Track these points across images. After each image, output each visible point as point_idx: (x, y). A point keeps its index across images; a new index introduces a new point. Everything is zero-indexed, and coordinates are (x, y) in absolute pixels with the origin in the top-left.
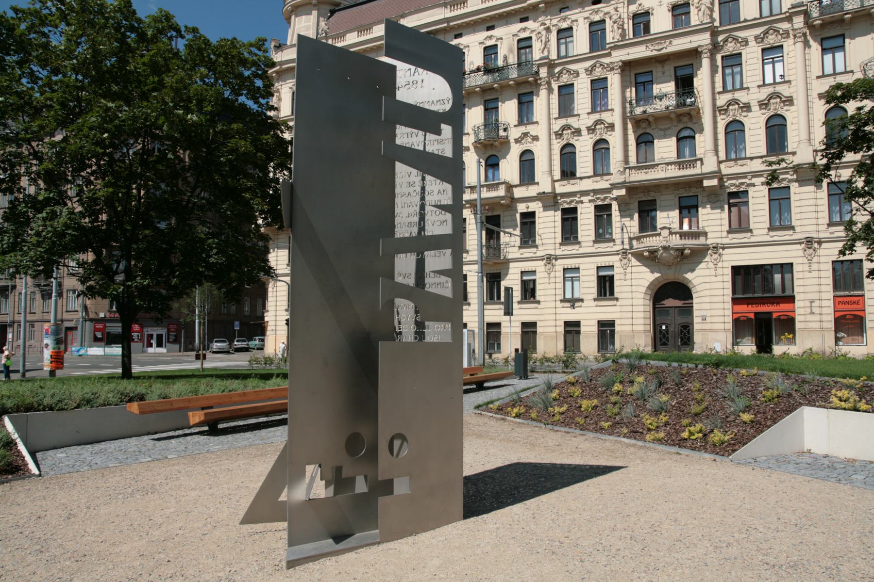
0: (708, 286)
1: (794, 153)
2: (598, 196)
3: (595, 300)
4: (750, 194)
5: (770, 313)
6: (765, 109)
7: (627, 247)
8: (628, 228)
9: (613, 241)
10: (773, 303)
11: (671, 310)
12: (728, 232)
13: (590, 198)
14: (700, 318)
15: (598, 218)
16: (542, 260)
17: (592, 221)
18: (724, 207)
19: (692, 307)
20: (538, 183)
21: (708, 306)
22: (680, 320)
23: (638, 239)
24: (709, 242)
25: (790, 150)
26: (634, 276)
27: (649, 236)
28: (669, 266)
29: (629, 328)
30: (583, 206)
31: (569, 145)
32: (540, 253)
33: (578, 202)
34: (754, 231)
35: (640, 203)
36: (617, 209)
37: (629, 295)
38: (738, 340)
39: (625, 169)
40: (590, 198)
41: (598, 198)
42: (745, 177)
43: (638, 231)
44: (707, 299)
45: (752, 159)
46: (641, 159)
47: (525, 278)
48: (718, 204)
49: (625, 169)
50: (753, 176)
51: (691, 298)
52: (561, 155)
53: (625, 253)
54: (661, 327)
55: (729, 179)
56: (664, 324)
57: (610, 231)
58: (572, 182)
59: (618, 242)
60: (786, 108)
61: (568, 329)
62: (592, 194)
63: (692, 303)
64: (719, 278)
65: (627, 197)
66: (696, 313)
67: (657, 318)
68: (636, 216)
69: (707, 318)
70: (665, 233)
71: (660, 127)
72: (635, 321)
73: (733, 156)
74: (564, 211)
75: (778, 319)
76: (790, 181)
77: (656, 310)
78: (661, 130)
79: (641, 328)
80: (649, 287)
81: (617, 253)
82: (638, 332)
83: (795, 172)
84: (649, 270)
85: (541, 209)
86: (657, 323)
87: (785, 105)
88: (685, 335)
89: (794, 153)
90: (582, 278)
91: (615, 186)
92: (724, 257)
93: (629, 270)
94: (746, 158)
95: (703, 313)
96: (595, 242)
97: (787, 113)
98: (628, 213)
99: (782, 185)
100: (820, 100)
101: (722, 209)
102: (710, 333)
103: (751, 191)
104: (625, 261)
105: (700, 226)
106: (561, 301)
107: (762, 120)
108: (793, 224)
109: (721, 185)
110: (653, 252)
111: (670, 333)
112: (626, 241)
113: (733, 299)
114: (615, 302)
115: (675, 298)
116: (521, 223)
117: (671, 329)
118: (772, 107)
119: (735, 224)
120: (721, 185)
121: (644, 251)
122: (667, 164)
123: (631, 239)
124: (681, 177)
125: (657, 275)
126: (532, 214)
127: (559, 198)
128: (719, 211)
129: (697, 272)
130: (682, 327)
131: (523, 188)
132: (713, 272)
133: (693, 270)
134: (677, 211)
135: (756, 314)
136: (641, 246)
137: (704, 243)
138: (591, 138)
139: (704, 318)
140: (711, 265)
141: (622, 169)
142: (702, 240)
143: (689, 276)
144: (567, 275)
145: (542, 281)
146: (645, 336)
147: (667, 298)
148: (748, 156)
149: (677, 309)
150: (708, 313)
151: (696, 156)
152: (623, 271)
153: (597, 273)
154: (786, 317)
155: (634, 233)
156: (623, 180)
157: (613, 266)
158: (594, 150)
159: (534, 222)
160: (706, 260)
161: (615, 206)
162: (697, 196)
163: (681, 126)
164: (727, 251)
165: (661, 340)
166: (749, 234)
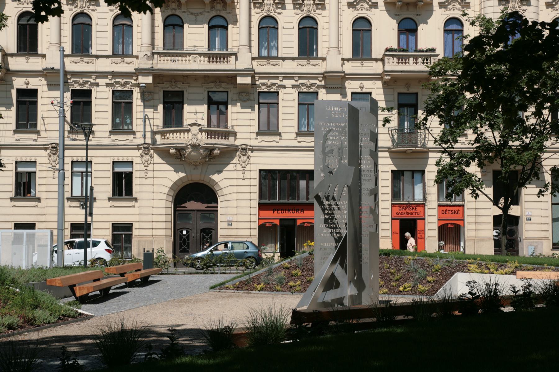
0: (235, 189)
1: (324, 59)
2: (117, 80)
3: (110, 199)
4: (281, 96)
5: (294, 220)
6: (299, 9)
7: (149, 141)
8: (151, 121)
9: (134, 133)
10: (297, 210)
11: (192, 215)
12: (258, 134)
13: (107, 81)
14: (226, 223)
15: (116, 106)
16: (46, 149)
17: (109, 108)
18: (254, 107)
19: (217, 211)
20: (44, 56)
21: (234, 211)
22: (203, 225)
23: (162, 133)
24: (238, 143)
25: (320, 56)
26: (156, 174)
27: (173, 132)
28: (196, 165)
29: (149, 233)
31: (82, 14)
32: (41, 141)
33: (93, 85)
34: (283, 135)
35: (166, 93)
36: (139, 97)
38: (263, 247)
39: (153, 54)
40: (107, 81)
41: (117, 83)
42: (277, 78)
43: (162, 125)
44: (234, 204)
45: (284, 59)
46: (169, 44)
47: (20, 169)
48: (248, 103)
49: (153, 54)
50: (285, 78)
51: (217, 202)
52: (72, 25)
53: (147, 148)
54: (182, 232)
55: (261, 78)
56: (184, 229)
57: (128, 121)
58: (86, 59)
59: (139, 135)
60: (318, 11)
62: (110, 77)
63: (217, 207)
64: (247, 182)
65: (152, 85)
66: (220, 218)
67: (178, 222)
68: (160, 107)
70: (195, 129)
71: (191, 10)
72: (155, 225)
73: (265, 53)
74: (75, 93)
75: (302, 226)
76: (319, 87)
77: (177, 213)
78: (192, 14)
79: (162, 233)
80: (171, 188)
82: (159, 237)
83: (324, 78)
84: (173, 169)
85: (46, 88)
86: (178, 227)
87: (317, 8)
89: (324, 59)
91: (139, 72)
92: (253, 160)
93: (151, 167)
94: (277, 58)
95: (229, 218)
96: (111, 133)
97: (319, 16)
98: (151, 103)
99: (311, 90)
100: (349, 8)
101: (253, 109)
103: (282, 92)
104: (147, 157)
105: (230, 124)
106: (68, 199)
107: (297, 19)
108: (280, 131)
109: (253, 84)
110: (180, 150)
111: (191, 238)
112: (148, 135)
113: (259, 204)
114: (133, 203)
115: (197, 201)
116: (18, 102)
117: (193, 234)
118: (306, 9)
119: (264, 127)
120: (253, 84)
121: (170, 148)
122: (200, 54)
123: (154, 133)
125: (182, 175)
126: (34, 92)
127: (69, 77)
128: (249, 110)
129: (224, 174)
131: (22, 59)
132: (241, 176)
133: (220, 172)
134: (206, 106)
135: (281, 220)
136: (166, 141)
137: (233, 143)
138: (111, 11)
139: (230, 224)
140: (239, 167)
142: (231, 141)
143: (216, 177)
144: (75, 169)
145: (44, 174)
146: (166, 241)
148: (279, 56)
150: (235, 218)
151: (227, 50)
152: (144, 168)
153: (113, 169)
155: (158, 126)
156: (150, 66)
157: (132, 162)
158: (114, 26)
159: (35, 103)
160: (234, 161)
161: (137, 94)
162: (227, 92)
163: (214, 13)
164: (255, 154)
165: (181, 246)
166: (277, 138)
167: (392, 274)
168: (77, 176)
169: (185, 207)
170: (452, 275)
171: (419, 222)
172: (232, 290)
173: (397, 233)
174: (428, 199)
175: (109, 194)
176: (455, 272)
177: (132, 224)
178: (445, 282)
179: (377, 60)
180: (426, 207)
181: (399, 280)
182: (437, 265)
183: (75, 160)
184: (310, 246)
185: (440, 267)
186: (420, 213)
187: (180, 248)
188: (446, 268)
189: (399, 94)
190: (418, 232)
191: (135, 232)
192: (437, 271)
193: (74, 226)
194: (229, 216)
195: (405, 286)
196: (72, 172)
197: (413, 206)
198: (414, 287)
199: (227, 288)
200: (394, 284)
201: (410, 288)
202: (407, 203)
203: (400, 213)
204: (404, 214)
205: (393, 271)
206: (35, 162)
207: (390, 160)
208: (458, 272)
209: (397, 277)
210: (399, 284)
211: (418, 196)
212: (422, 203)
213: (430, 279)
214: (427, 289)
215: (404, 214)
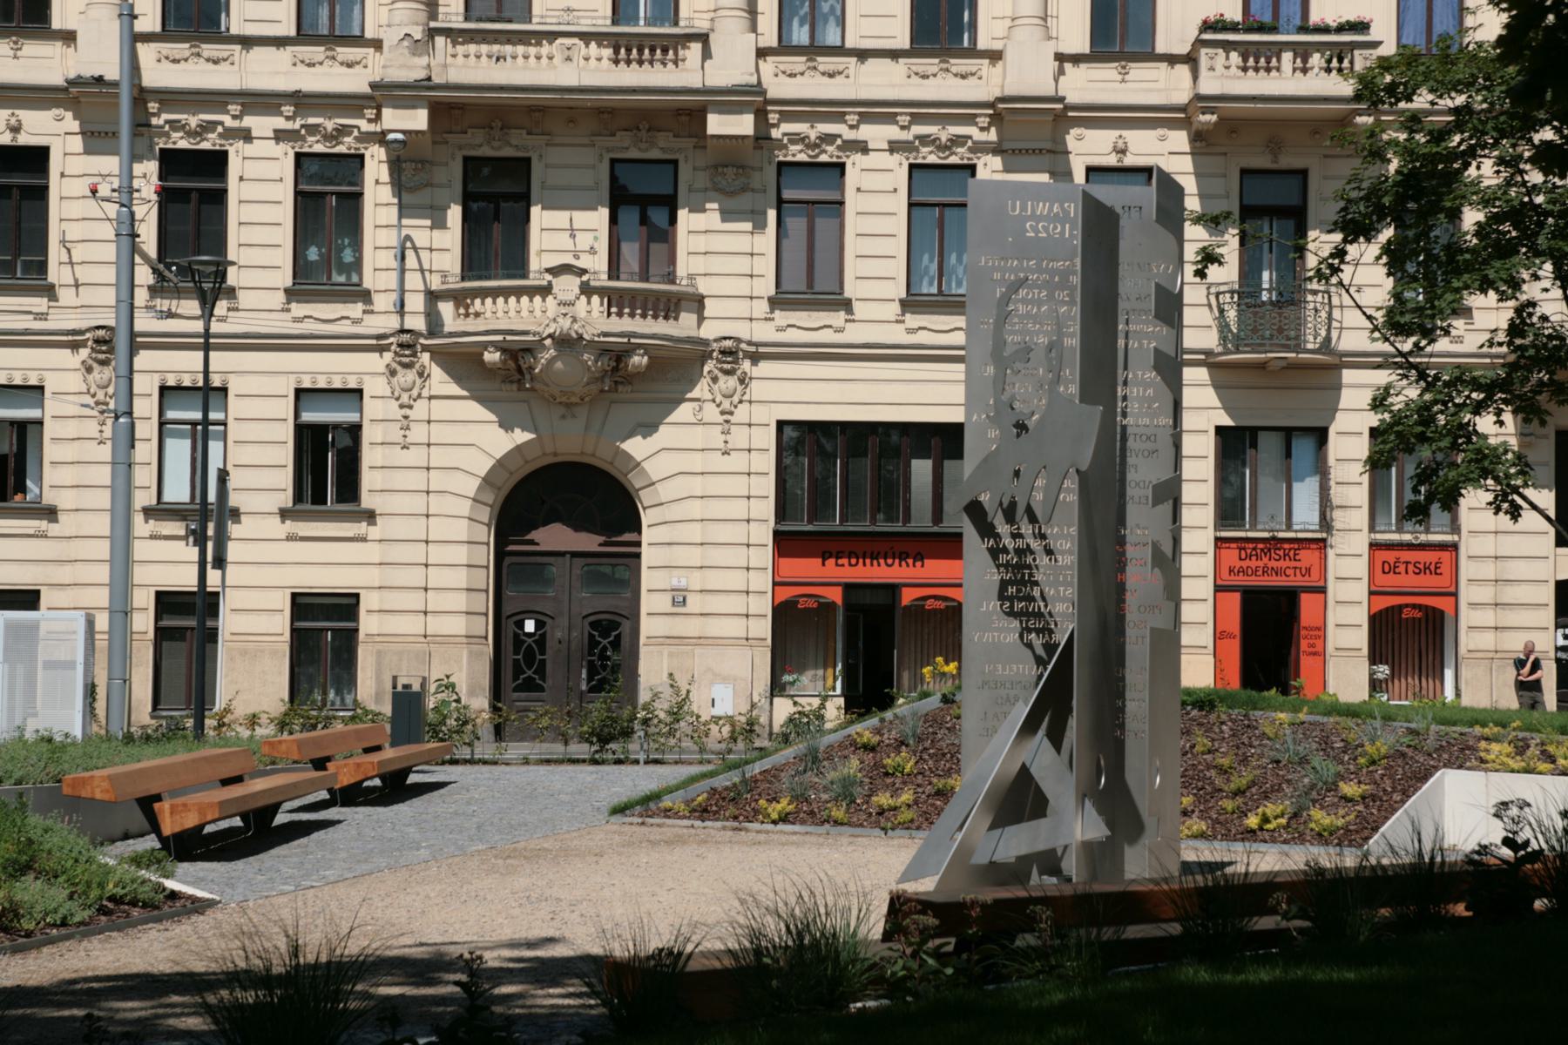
0: (697, 485)
1: (995, 56)
2: (312, 121)
3: (284, 514)
5: (893, 589)
7: (417, 323)
8: (424, 255)
9: (366, 296)
10: (902, 556)
11: (556, 569)
12: (775, 303)
13: (280, 123)
14: (668, 598)
15: (307, 206)
16: (75, 346)
17: (285, 214)
18: (765, 213)
19: (638, 556)
20: (69, 37)
21: (694, 556)
22: (590, 601)
23: (459, 298)
24: (709, 331)
25: (982, 44)
26: (439, 433)
27: (495, 293)
28: (568, 405)
29: (413, 625)
30: (249, 150)
32: (61, 321)
34: (856, 306)
35: (472, 165)
36: (385, 176)
37: (417, 504)
38: (787, 678)
39: (432, 33)
40: (280, 123)
41: (312, 129)
42: (840, 118)
43: (457, 269)
44: (694, 533)
45: (863, 55)
48: (745, 201)
49: (432, 33)
50: (865, 118)
51: (638, 528)
53: (406, 346)
54: (521, 625)
55: (786, 117)
56: (529, 613)
57: (348, 256)
58: (209, 49)
59: (383, 302)
61: (166, 622)
62: (288, 110)
63: (639, 544)
64: (737, 462)
65: (428, 136)
66: (648, 579)
67: (508, 593)
68: (455, 214)
69: (691, 598)
70: (567, 286)
72: (435, 601)
73: (800, 35)
74: (172, 162)
76: (980, 148)
77: (508, 561)
79: (457, 626)
80: (488, 481)
81: (378, 344)
82: (446, 639)
83: (997, 119)
84: (493, 418)
85: (77, 143)
86: (508, 609)
88: (603, 657)
89: (995, 56)
90: (234, 431)
91: (384, 94)
92: (757, 390)
93: (420, 410)
94: (840, 51)
96: (292, 294)
98: (423, 197)
99: (953, 160)
102: (698, 650)
103: (855, 165)
104: (409, 376)
105: (682, 270)
106: (148, 512)
108: (848, 293)
109: (762, 137)
110: (518, 354)
111: (551, 644)
112: (416, 302)
113: (776, 534)
114: (361, 528)
117: (556, 633)
119: (795, 281)
120: (762, 137)
121: (485, 345)
122: (586, 37)
123: (433, 297)
124: (634, 91)
125: (521, 436)
127: (153, 106)
128: (748, 226)
129: (665, 435)
130: (593, 625)
132: (715, 437)
134: (603, 213)
135: (849, 588)
136: (471, 325)
137: (693, 333)
139: (679, 598)
140: (711, 413)
141: (418, 33)
142: (685, 325)
143: (635, 447)
144: (171, 415)
145: (71, 429)
146: (470, 653)
147: (545, 524)
148: (849, 44)
149: (579, 562)
150: (695, 580)
151: (676, 24)
152: (399, 414)
153: (297, 415)
154: (942, 605)
155: (444, 275)
156: (422, 74)
157: (359, 392)
159: (42, 193)
161: (376, 167)
162: (675, 163)
164: (765, 368)
165: (518, 671)
166: (838, 318)
167: (1223, 771)
168: (180, 435)
169: (532, 542)
170: (1425, 778)
171: (1306, 600)
172: (684, 817)
173: (1231, 636)
174: (1337, 525)
175: (282, 496)
176: (1436, 768)
177: (357, 596)
178: (1403, 802)
179: (1172, 60)
180: (1331, 553)
181: (1244, 792)
182: (1373, 742)
183: (171, 382)
184: (944, 674)
185: (1383, 750)
186: (1308, 570)
187: (516, 678)
188: (1403, 755)
189: (1245, 172)
190: (1303, 633)
191: (367, 624)
192: (1373, 762)
193: (167, 602)
194: (676, 572)
195: (1264, 814)
196: (162, 424)
197: (1286, 546)
198: (1295, 815)
199: (667, 813)
200: (1229, 805)
201: (1283, 821)
202: (1266, 535)
203: (1242, 571)
204: (1255, 572)
205: (1225, 762)
206: (41, 388)
207: (1211, 391)
208: (1445, 766)
209: (1238, 782)
210: (1246, 804)
211: (1305, 514)
212: (1318, 536)
213: (1349, 789)
214: (1340, 822)
215: (1255, 572)
